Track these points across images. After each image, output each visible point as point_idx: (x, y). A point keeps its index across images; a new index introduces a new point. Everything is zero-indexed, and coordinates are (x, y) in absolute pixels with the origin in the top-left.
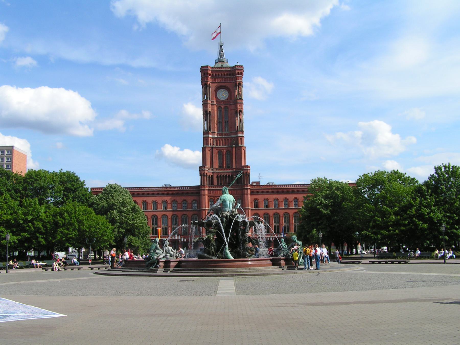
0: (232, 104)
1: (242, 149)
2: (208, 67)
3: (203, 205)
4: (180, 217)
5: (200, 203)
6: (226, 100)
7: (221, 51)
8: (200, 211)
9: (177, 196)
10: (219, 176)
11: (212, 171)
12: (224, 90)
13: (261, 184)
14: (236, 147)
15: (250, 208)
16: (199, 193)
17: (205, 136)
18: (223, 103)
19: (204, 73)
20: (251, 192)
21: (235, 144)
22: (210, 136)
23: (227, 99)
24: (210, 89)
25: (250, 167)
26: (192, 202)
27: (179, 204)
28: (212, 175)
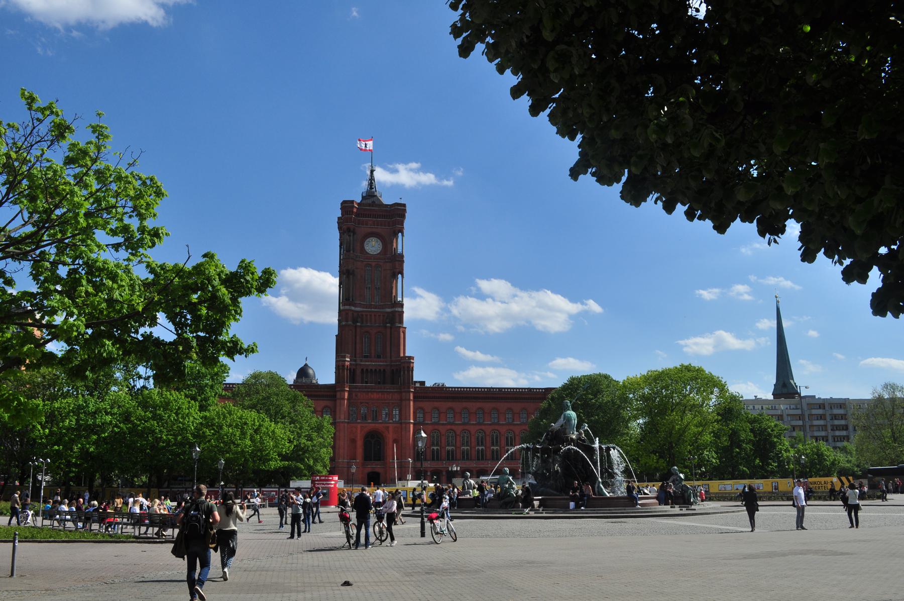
3: (342, 417)
6: (378, 254)
14: (391, 328)
15: (412, 421)
16: (335, 396)
20: (414, 397)
21: (389, 323)
22: (353, 308)
25: (413, 359)
26: (323, 409)
28: (354, 370)
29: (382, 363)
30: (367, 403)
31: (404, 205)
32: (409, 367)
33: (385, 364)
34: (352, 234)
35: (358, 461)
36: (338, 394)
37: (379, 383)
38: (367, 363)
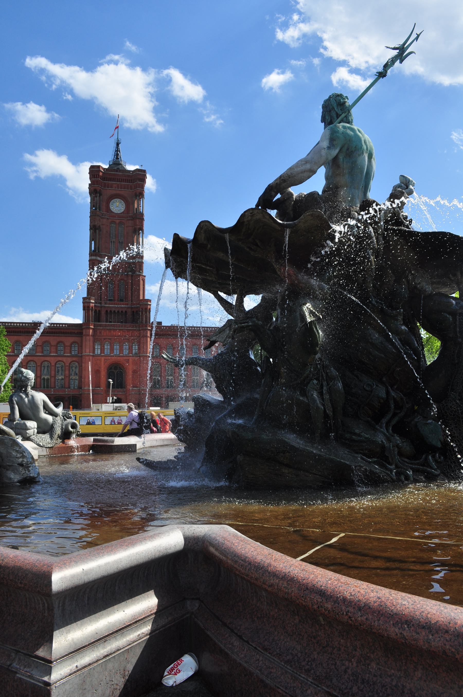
0: (129, 220)
1: (141, 279)
2: (100, 168)
3: (88, 350)
4: (53, 364)
5: (82, 346)
6: (121, 213)
7: (117, 150)
8: (81, 356)
9: (51, 336)
10: (109, 311)
11: (99, 305)
12: (119, 200)
13: (163, 325)
14: (132, 276)
17: (94, 258)
18: (118, 217)
19: (94, 175)
21: (131, 272)
23: (123, 212)
24: (101, 197)
25: (150, 302)
27: (52, 347)
28: (99, 311)
29: (124, 306)
30: (110, 339)
31: (144, 171)
32: (146, 309)
33: (127, 306)
34: (98, 195)
35: (102, 388)
36: (84, 331)
37: (122, 322)
38: (111, 306)
